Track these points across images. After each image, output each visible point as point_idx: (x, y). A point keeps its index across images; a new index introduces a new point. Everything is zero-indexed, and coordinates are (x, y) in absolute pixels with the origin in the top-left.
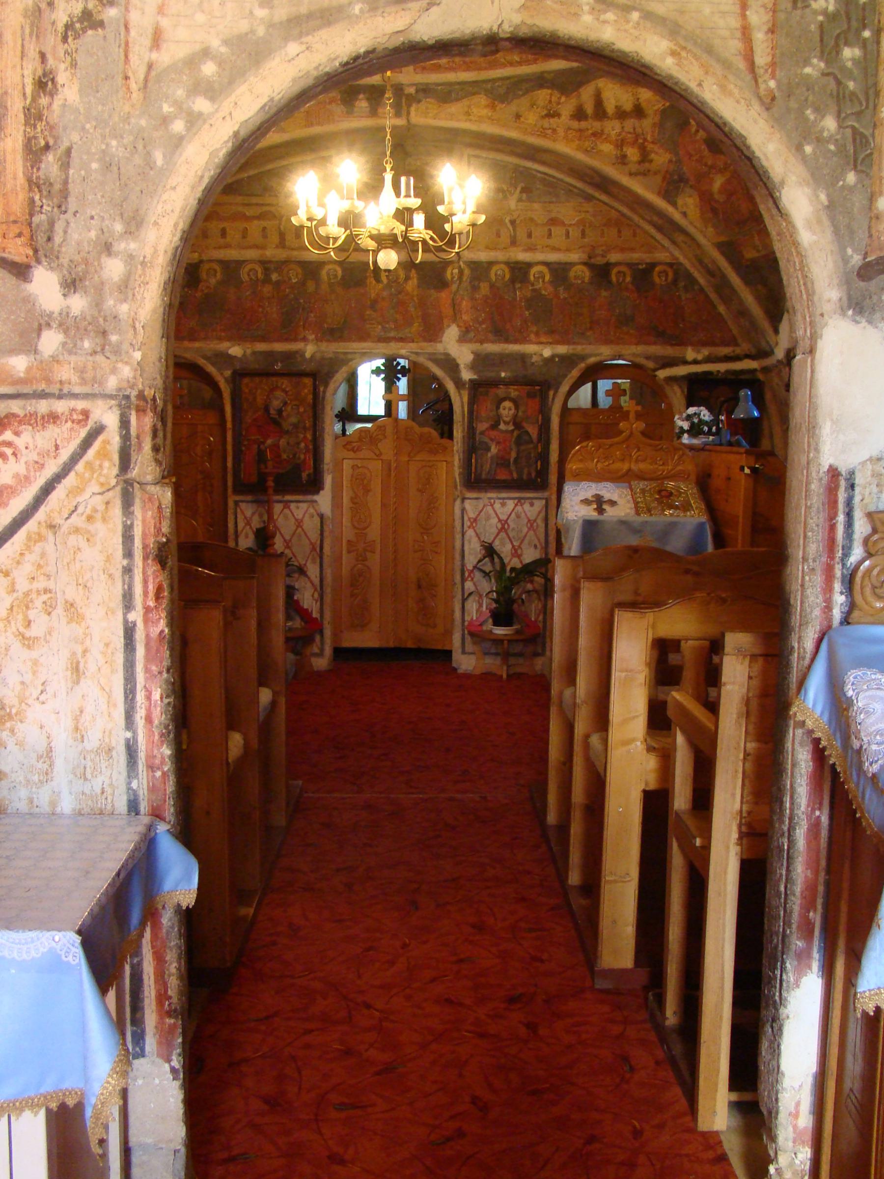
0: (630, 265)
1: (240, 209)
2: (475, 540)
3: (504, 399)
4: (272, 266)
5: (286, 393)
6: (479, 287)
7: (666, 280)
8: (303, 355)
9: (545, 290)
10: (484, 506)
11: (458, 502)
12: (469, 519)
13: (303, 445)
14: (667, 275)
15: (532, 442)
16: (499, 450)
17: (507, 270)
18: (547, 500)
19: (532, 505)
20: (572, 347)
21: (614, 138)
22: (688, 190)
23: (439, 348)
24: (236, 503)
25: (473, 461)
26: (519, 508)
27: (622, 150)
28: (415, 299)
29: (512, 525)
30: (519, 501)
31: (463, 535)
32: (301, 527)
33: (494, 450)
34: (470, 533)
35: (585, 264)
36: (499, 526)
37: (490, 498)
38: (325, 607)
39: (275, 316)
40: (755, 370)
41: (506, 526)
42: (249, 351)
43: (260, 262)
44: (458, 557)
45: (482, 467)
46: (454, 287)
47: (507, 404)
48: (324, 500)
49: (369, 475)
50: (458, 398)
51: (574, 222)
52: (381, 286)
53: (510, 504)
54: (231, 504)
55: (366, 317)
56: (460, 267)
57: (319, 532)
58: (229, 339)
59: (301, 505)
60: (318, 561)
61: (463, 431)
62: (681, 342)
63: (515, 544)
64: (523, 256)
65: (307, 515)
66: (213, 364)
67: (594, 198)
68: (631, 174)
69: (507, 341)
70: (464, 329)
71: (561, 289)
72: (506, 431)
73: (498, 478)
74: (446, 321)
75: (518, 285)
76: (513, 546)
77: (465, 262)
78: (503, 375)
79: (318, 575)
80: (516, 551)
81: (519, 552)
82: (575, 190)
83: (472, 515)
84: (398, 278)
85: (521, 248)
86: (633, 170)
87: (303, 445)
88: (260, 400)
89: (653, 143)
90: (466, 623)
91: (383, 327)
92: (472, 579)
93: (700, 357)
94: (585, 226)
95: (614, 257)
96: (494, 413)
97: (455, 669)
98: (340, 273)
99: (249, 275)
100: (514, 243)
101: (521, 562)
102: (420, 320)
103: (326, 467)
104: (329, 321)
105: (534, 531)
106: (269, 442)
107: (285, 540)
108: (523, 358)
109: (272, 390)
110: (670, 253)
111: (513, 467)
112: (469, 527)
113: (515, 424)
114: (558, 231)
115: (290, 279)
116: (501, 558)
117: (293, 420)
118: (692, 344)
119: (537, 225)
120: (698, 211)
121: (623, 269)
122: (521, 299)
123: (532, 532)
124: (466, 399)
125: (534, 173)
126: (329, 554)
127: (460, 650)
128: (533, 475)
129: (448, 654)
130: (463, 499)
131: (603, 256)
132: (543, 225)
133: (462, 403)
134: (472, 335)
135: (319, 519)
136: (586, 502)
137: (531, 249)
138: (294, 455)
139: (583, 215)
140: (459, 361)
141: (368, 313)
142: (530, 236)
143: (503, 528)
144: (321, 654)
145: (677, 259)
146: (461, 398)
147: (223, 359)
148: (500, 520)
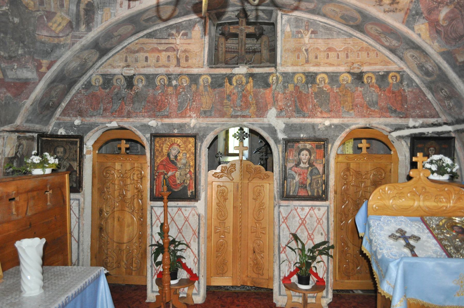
0: (373, 73)
1: (156, 46)
2: (286, 229)
3: (302, 150)
4: (172, 77)
5: (180, 146)
6: (288, 87)
8: (189, 126)
9: (326, 87)
10: (292, 210)
11: (277, 208)
12: (283, 217)
13: (188, 175)
14: (396, 77)
15: (319, 173)
16: (300, 179)
17: (303, 77)
18: (328, 207)
19: (319, 210)
20: (341, 119)
22: (422, 20)
23: (265, 121)
24: (152, 208)
25: (285, 184)
26: (312, 212)
28: (252, 94)
29: (308, 221)
30: (312, 208)
31: (279, 227)
32: (188, 221)
33: (297, 178)
34: (284, 225)
35: (349, 72)
36: (300, 222)
37: (295, 206)
38: (200, 266)
39: (174, 104)
40: (450, 132)
41: (304, 222)
42: (160, 124)
43: (166, 74)
44: (276, 239)
45: (290, 188)
46: (274, 87)
47: (305, 152)
48: (200, 205)
49: (226, 191)
50: (276, 149)
51: (342, 49)
52: (232, 87)
53: (307, 209)
54: (149, 208)
56: (277, 75)
57: (198, 224)
58: (150, 117)
59: (187, 209)
60: (197, 240)
61: (279, 167)
62: (406, 117)
63: (310, 232)
64: (313, 69)
65: (191, 215)
66: (140, 131)
67: (353, 35)
68: (385, 12)
69: (304, 117)
71: (335, 87)
72: (305, 168)
73: (299, 195)
74: (269, 107)
75: (310, 85)
76: (309, 234)
77: (280, 73)
78: (302, 136)
79: (197, 249)
80: (310, 236)
81: (312, 237)
82: (342, 32)
83: (284, 215)
84: (242, 82)
85: (312, 65)
86: (387, 9)
87: (188, 175)
88: (165, 151)
90: (282, 278)
91: (234, 110)
92: (285, 252)
93: (417, 125)
94: (348, 51)
95: (365, 68)
96: (297, 157)
97: (275, 305)
98: (210, 80)
99: (160, 82)
100: (307, 62)
101: (314, 243)
102: (255, 106)
103: (202, 188)
104: (204, 106)
105: (321, 225)
106: (170, 174)
107: (179, 229)
108: (313, 126)
109: (172, 145)
111: (308, 188)
112: (283, 222)
113: (309, 164)
114: (332, 55)
115: (182, 84)
116: (302, 242)
117: (184, 161)
118: (412, 117)
119: (321, 51)
120: (428, 33)
121: (370, 75)
122: (312, 93)
123: (320, 225)
124: (280, 150)
125: (319, 23)
126: (203, 237)
127: (278, 293)
128: (320, 192)
129: (270, 292)
130: (279, 206)
131: (358, 68)
132: (325, 51)
133: (279, 151)
134: (284, 113)
135: (197, 217)
136: (392, 236)
137: (317, 65)
138: (184, 181)
139: (346, 46)
140: (276, 128)
141: (225, 102)
142: (316, 57)
143: (302, 223)
144: (198, 294)
146: (278, 149)
147: (145, 127)
148: (301, 219)
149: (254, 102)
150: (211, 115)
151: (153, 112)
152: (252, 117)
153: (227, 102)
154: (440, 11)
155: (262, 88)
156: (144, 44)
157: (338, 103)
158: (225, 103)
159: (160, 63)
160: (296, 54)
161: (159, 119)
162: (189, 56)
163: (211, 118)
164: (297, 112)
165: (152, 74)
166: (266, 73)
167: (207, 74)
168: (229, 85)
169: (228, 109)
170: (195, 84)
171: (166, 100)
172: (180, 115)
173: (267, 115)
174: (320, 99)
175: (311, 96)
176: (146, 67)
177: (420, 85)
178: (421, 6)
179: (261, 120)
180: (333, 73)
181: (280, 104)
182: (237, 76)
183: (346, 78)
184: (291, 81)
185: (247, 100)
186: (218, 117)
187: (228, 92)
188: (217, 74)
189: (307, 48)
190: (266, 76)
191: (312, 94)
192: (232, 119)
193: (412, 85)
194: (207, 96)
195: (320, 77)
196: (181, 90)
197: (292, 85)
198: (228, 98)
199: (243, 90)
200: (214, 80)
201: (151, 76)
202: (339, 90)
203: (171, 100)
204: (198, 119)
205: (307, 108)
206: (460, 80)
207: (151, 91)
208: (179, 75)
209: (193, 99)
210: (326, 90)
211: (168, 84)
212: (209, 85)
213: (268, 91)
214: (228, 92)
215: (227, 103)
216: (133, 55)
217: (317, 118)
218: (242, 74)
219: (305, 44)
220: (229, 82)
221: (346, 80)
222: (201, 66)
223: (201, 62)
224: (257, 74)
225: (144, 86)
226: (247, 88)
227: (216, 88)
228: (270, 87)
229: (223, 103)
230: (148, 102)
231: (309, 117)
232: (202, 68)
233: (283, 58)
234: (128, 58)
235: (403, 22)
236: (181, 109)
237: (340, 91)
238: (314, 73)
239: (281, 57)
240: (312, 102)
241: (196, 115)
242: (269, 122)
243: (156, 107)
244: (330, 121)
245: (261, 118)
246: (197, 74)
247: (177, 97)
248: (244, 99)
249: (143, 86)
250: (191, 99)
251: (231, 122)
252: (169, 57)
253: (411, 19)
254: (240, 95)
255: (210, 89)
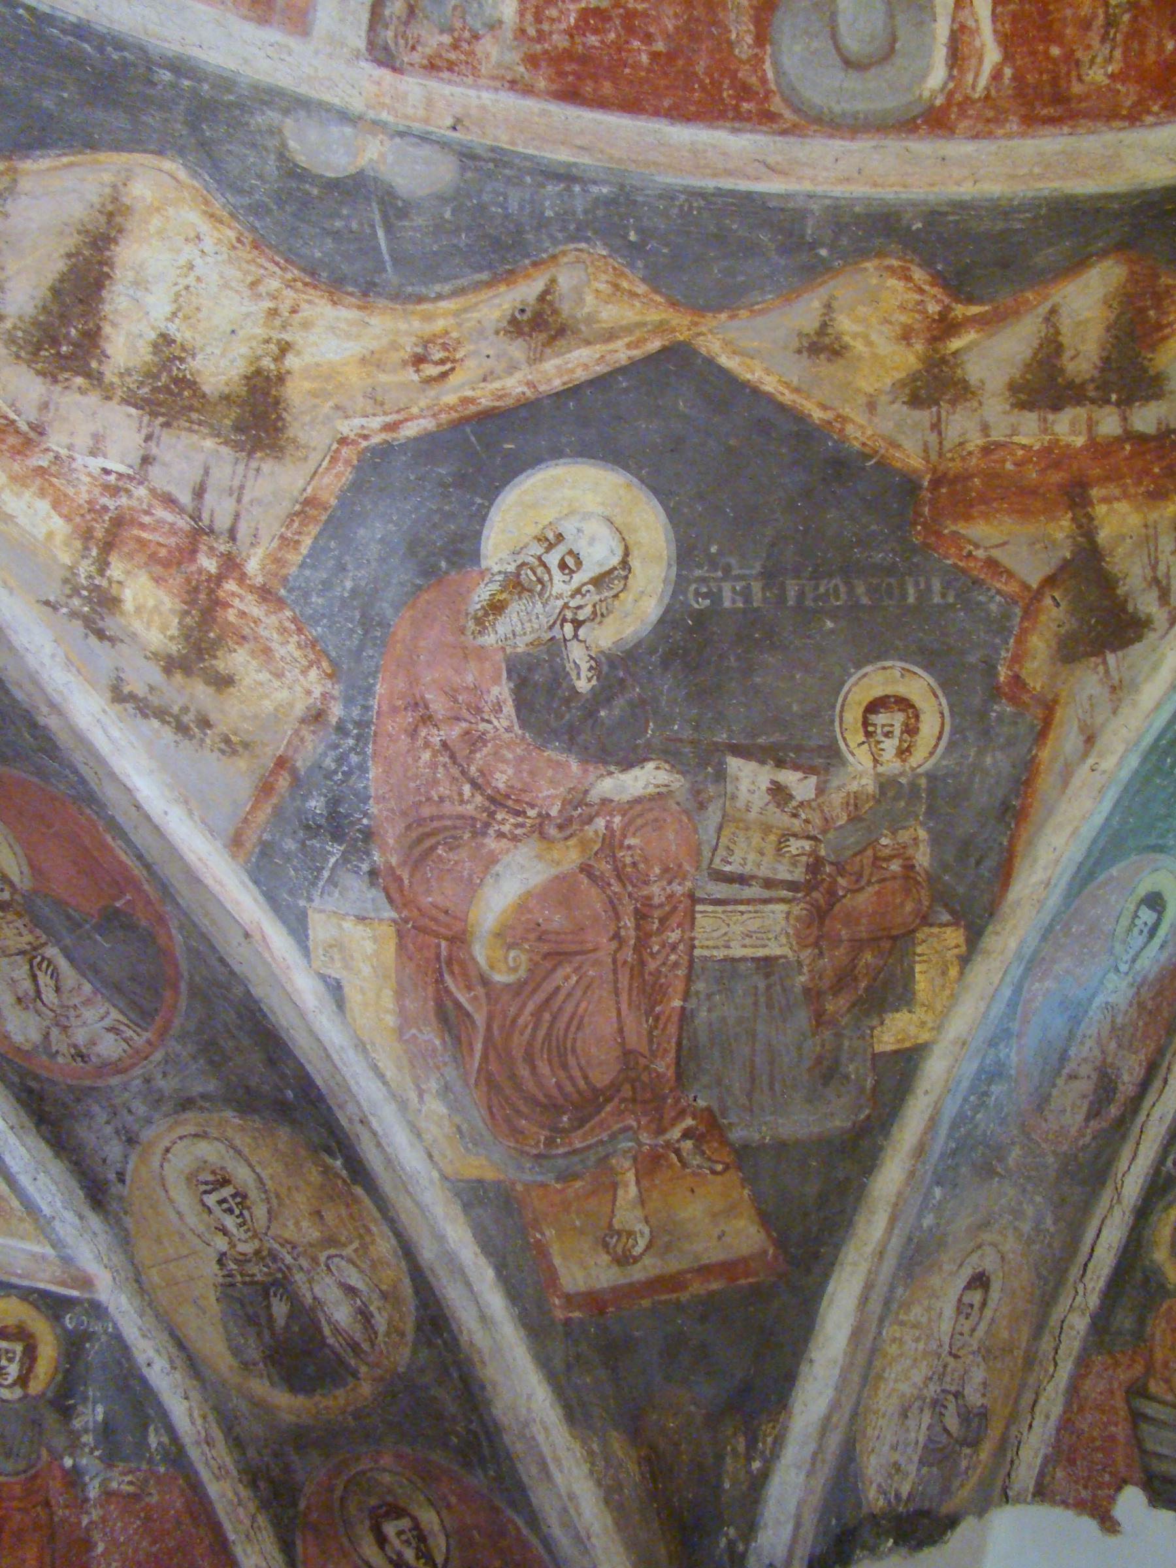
7: (23, 1380)
14: (30, 1353)
21: (82, 493)
22: (356, 888)
27: (103, 566)
68: (119, 695)
89: (265, 594)
110: (56, 1244)
120: (388, 999)
145: (86, 1282)
154: (493, 860)
177: (194, 1453)
178: (374, 772)
193: (143, 1442)
206: (576, 1446)
235: (236, 843)
253: (290, 845)
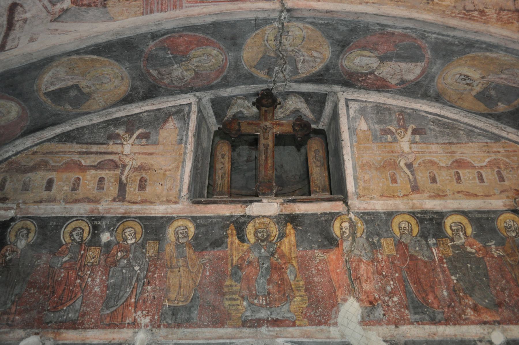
1: (76, 157)
6: (381, 246)
9: (471, 246)
17: (413, 222)
28: (295, 264)
43: (89, 218)
46: (346, 245)
51: (484, 164)
52: (246, 246)
55: (225, 290)
56: (351, 219)
69: (434, 321)
70: (367, 304)
77: (357, 214)
82: (476, 130)
84: (269, 236)
85: (426, 195)
91: (251, 304)
94: (499, 168)
98: (192, 230)
99: (71, 235)
100: (415, 189)
102: (303, 293)
115: (125, 239)
119: (440, 168)
122: (441, 260)
125: (425, 114)
132: (449, 168)
134: (379, 312)
139: (493, 156)
141: (228, 283)
142: (434, 180)
149: (302, 283)
150: (188, 320)
151: (39, 313)
152: (297, 323)
153: (234, 283)
155: (317, 249)
156: (51, 153)
157: (512, 284)
158: (227, 286)
159: (81, 193)
160: (389, 175)
161: (50, 331)
162: (148, 178)
163: (190, 327)
164: (415, 308)
165: (56, 217)
166: (325, 214)
167: (186, 218)
168: (237, 241)
169: (235, 303)
170: (156, 239)
171: (79, 281)
172: (107, 321)
173: (336, 317)
174: (464, 274)
175: (441, 267)
176: (45, 202)
179: (322, 330)
180: (480, 212)
181: (368, 288)
182: (257, 221)
183: (512, 223)
184: (387, 231)
185: (283, 280)
186: (207, 326)
187: (235, 259)
188: (210, 217)
189: (408, 162)
190: (326, 221)
191: (443, 263)
192: (244, 330)
194: (182, 268)
195: (451, 221)
196: (119, 254)
197: (390, 241)
198: (234, 274)
199: (273, 255)
200: (203, 229)
201: (52, 223)
202: (504, 251)
203: (90, 279)
204: (154, 330)
205: (436, 297)
207: (44, 258)
208: (119, 219)
209: (146, 277)
210: (474, 251)
211: (91, 241)
212: (188, 242)
213: (333, 255)
214: (235, 259)
215: (232, 286)
216: (20, 177)
217: (467, 324)
218: (269, 217)
219: (403, 154)
220: (238, 234)
221: (513, 228)
222: (174, 200)
223: (174, 192)
224: (303, 215)
225: (30, 246)
226: (283, 248)
227: (205, 249)
228: (337, 245)
229: (221, 287)
230: (32, 285)
231: (447, 322)
232: (176, 203)
233: (361, 183)
234: (7, 183)
236: (112, 303)
237: (508, 255)
238: (437, 213)
239: (356, 179)
240: (445, 281)
241: (151, 321)
242: (343, 336)
243: (50, 298)
244: (504, 331)
245: (323, 327)
246: (162, 218)
247: (106, 272)
248: (275, 277)
249: (28, 245)
250: (142, 276)
251: (241, 338)
252: (102, 180)
254: (265, 266)
255: (191, 251)
